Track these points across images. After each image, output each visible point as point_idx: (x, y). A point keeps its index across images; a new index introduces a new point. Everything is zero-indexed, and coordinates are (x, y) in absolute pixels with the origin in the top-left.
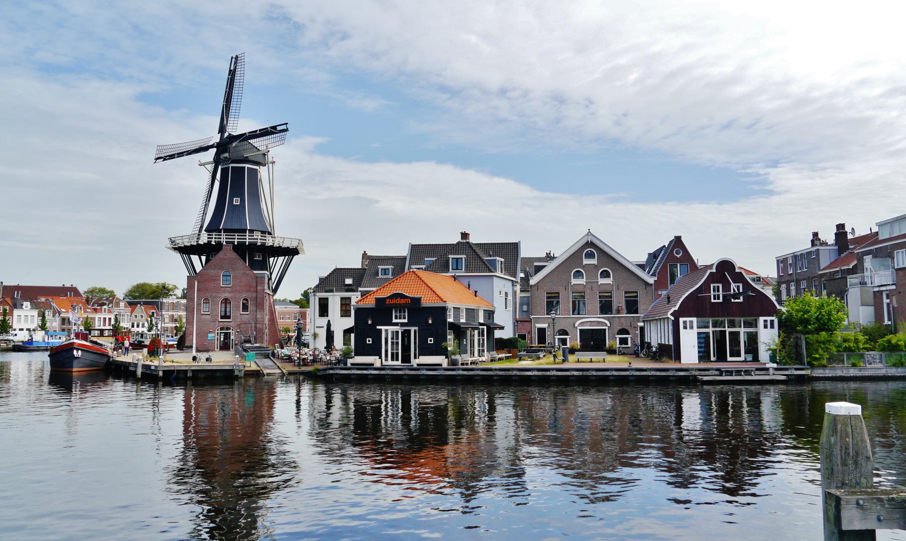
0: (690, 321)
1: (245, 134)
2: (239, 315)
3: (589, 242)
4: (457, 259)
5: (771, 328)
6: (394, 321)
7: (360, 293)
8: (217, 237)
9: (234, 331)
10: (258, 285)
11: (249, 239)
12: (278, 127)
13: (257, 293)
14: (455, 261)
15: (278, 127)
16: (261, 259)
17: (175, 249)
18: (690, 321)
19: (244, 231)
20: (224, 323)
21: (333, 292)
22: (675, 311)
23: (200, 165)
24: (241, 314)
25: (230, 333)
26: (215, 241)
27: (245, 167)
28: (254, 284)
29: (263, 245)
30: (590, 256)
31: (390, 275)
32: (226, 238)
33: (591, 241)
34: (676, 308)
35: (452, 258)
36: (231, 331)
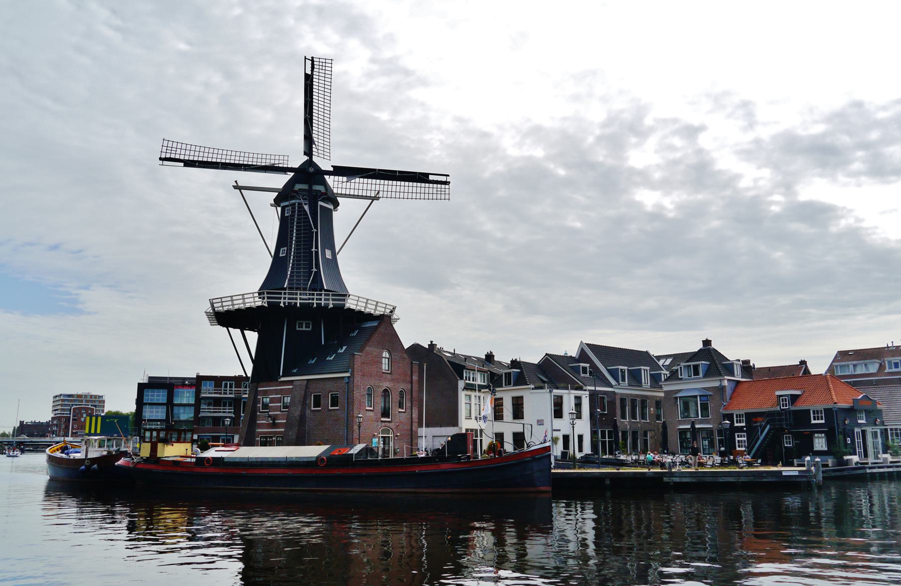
1: (376, 169)
2: (397, 412)
7: (588, 393)
8: (295, 296)
9: (392, 435)
10: (413, 374)
12: (430, 176)
13: (412, 384)
15: (430, 176)
20: (386, 424)
21: (568, 390)
23: (235, 187)
24: (399, 412)
25: (389, 437)
26: (284, 303)
28: (409, 373)
31: (588, 374)
36: (390, 435)
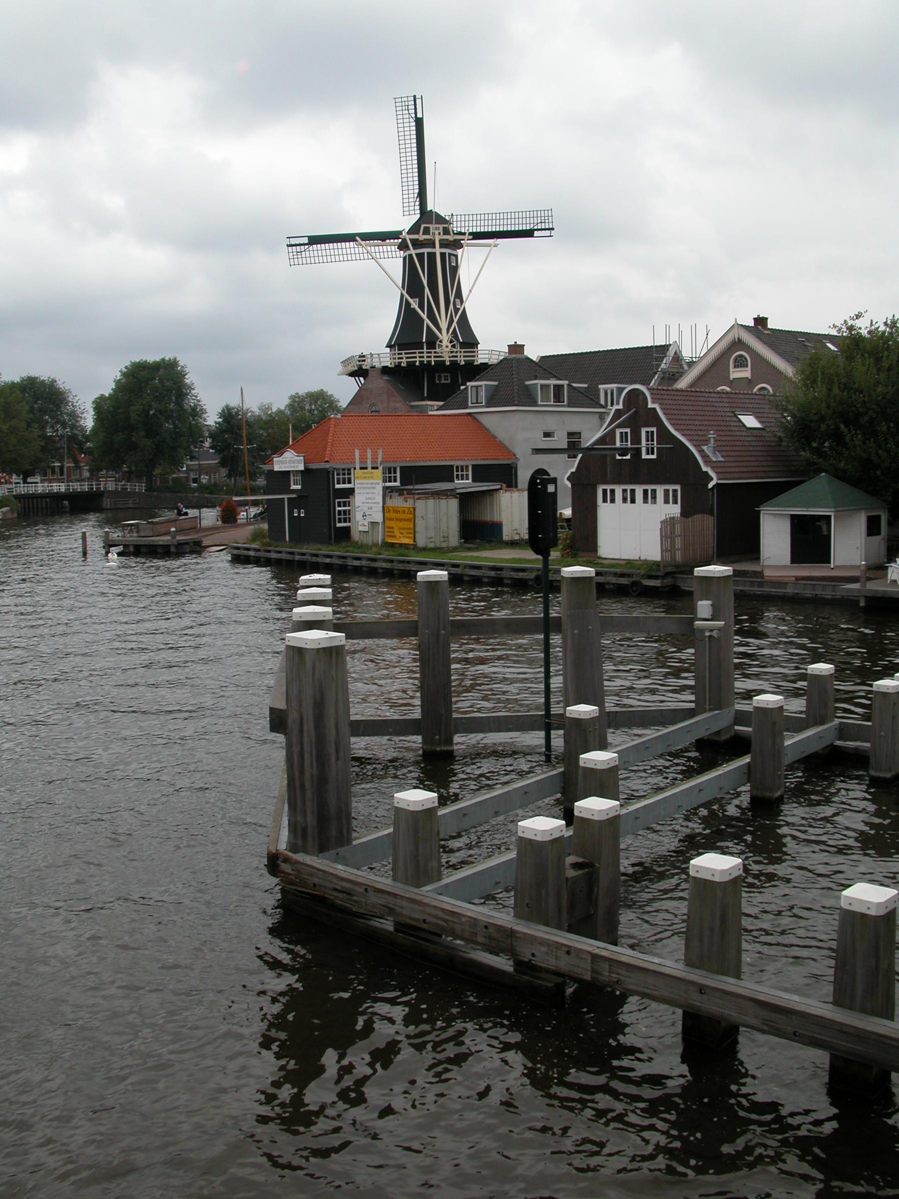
0: (652, 490)
3: (737, 340)
4: (477, 387)
5: (673, 503)
6: (293, 487)
11: (427, 357)
14: (474, 389)
16: (449, 381)
17: (352, 374)
18: (652, 490)
19: (419, 346)
22: (572, 473)
27: (424, 253)
29: (454, 364)
30: (740, 363)
32: (407, 358)
33: (739, 338)
34: (574, 470)
35: (472, 387)
